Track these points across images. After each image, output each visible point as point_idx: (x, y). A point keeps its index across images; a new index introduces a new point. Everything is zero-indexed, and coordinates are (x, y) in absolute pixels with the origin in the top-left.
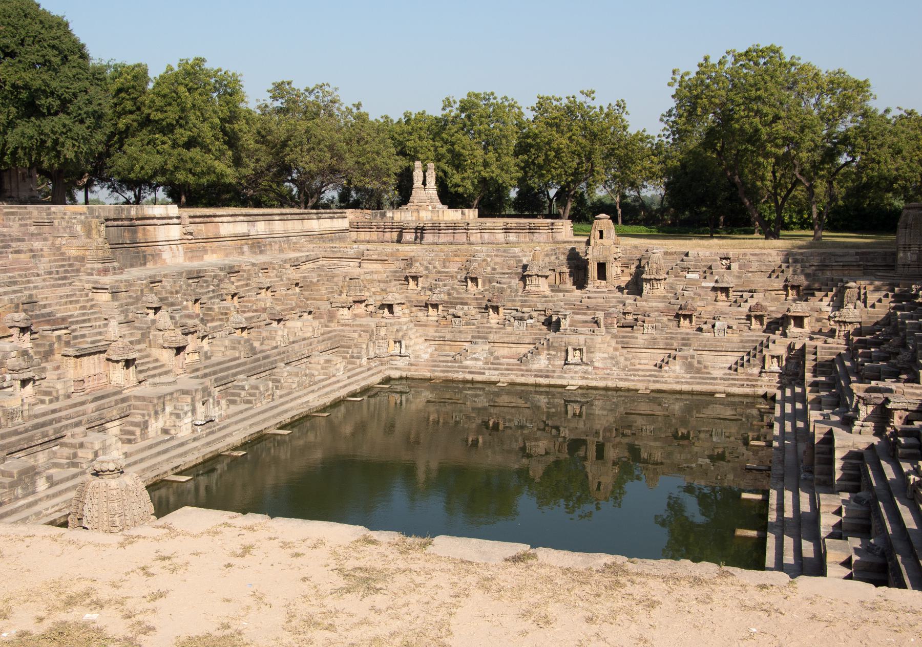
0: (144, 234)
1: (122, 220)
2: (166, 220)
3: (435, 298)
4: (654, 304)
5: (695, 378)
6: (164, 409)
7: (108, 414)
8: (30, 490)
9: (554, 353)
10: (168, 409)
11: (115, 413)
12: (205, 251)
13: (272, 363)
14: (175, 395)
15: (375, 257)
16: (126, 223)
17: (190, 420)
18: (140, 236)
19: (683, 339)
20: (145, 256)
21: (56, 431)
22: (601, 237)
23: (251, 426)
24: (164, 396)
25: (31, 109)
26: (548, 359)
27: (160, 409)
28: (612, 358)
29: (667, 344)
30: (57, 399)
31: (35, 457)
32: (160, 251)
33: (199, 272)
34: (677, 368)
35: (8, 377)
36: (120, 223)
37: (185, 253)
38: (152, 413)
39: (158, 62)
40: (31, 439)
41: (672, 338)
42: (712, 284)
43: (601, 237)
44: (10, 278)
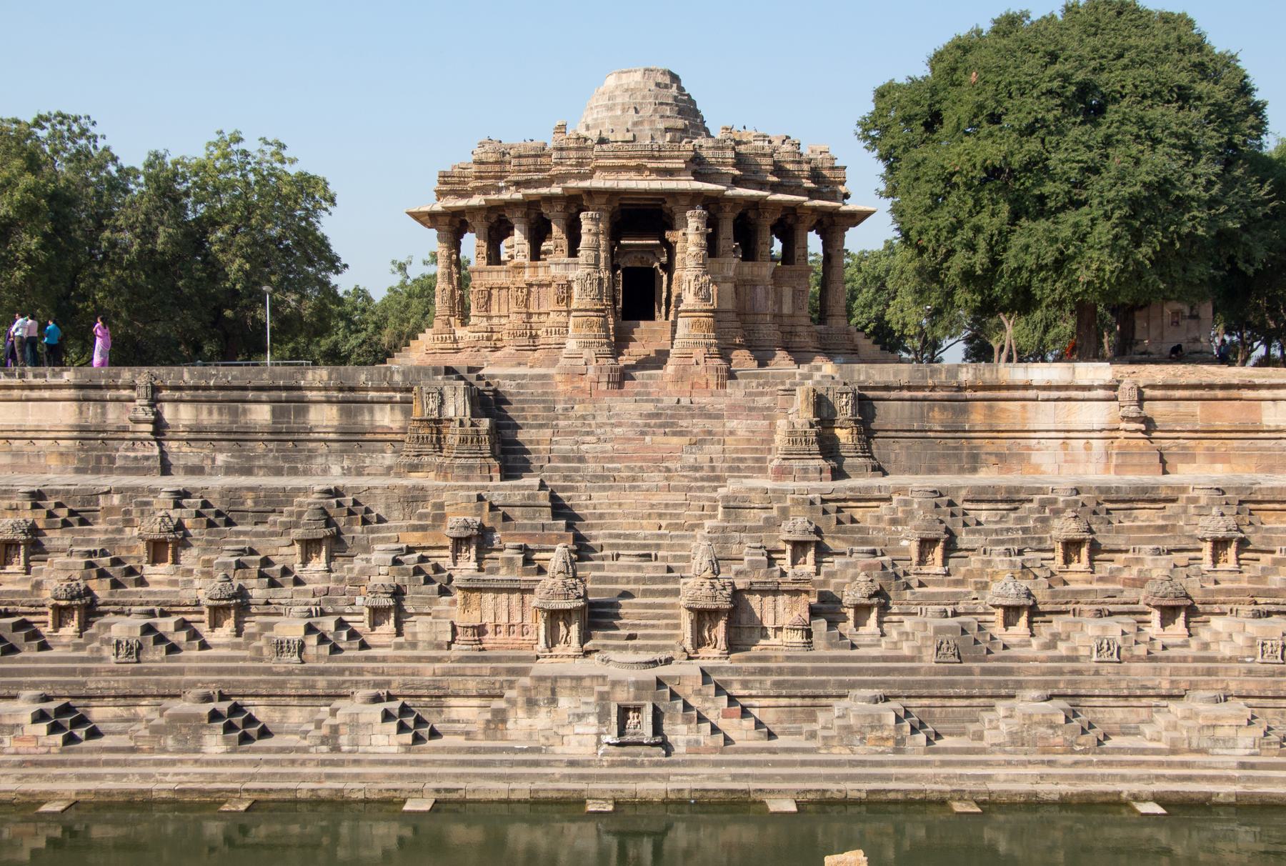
0: (991, 413)
1: (933, 388)
2: (1065, 392)
6: (553, 701)
7: (454, 684)
8: (191, 744)
10: (565, 703)
11: (472, 685)
12: (1188, 457)
13: (1005, 684)
14: (587, 683)
16: (939, 394)
17: (594, 730)
18: (977, 416)
21: (330, 684)
23: (735, 777)
24: (555, 679)
25: (1027, 207)
27: (542, 698)
30: (414, 645)
31: (285, 712)
32: (1029, 448)
33: (1018, 490)
35: (359, 600)
36: (920, 394)
37: (1108, 455)
38: (521, 700)
39: (187, 145)
40: (282, 684)
44: (609, 470)
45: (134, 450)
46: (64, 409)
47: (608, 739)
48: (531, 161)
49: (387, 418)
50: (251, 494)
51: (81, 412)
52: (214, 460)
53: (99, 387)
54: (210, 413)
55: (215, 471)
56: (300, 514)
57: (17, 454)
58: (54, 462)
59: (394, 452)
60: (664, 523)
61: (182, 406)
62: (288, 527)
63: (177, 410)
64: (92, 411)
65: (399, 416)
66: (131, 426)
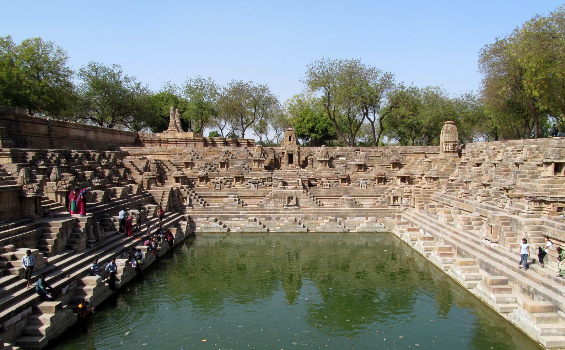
3: (201, 173)
4: (325, 174)
5: (356, 210)
6: (67, 232)
9: (277, 200)
15: (162, 153)
19: (345, 191)
20: (26, 142)
22: (290, 140)
26: (274, 204)
28: (310, 201)
29: (337, 193)
34: (346, 205)
41: (339, 190)
42: (353, 163)
43: (290, 140)
47: (92, 241)
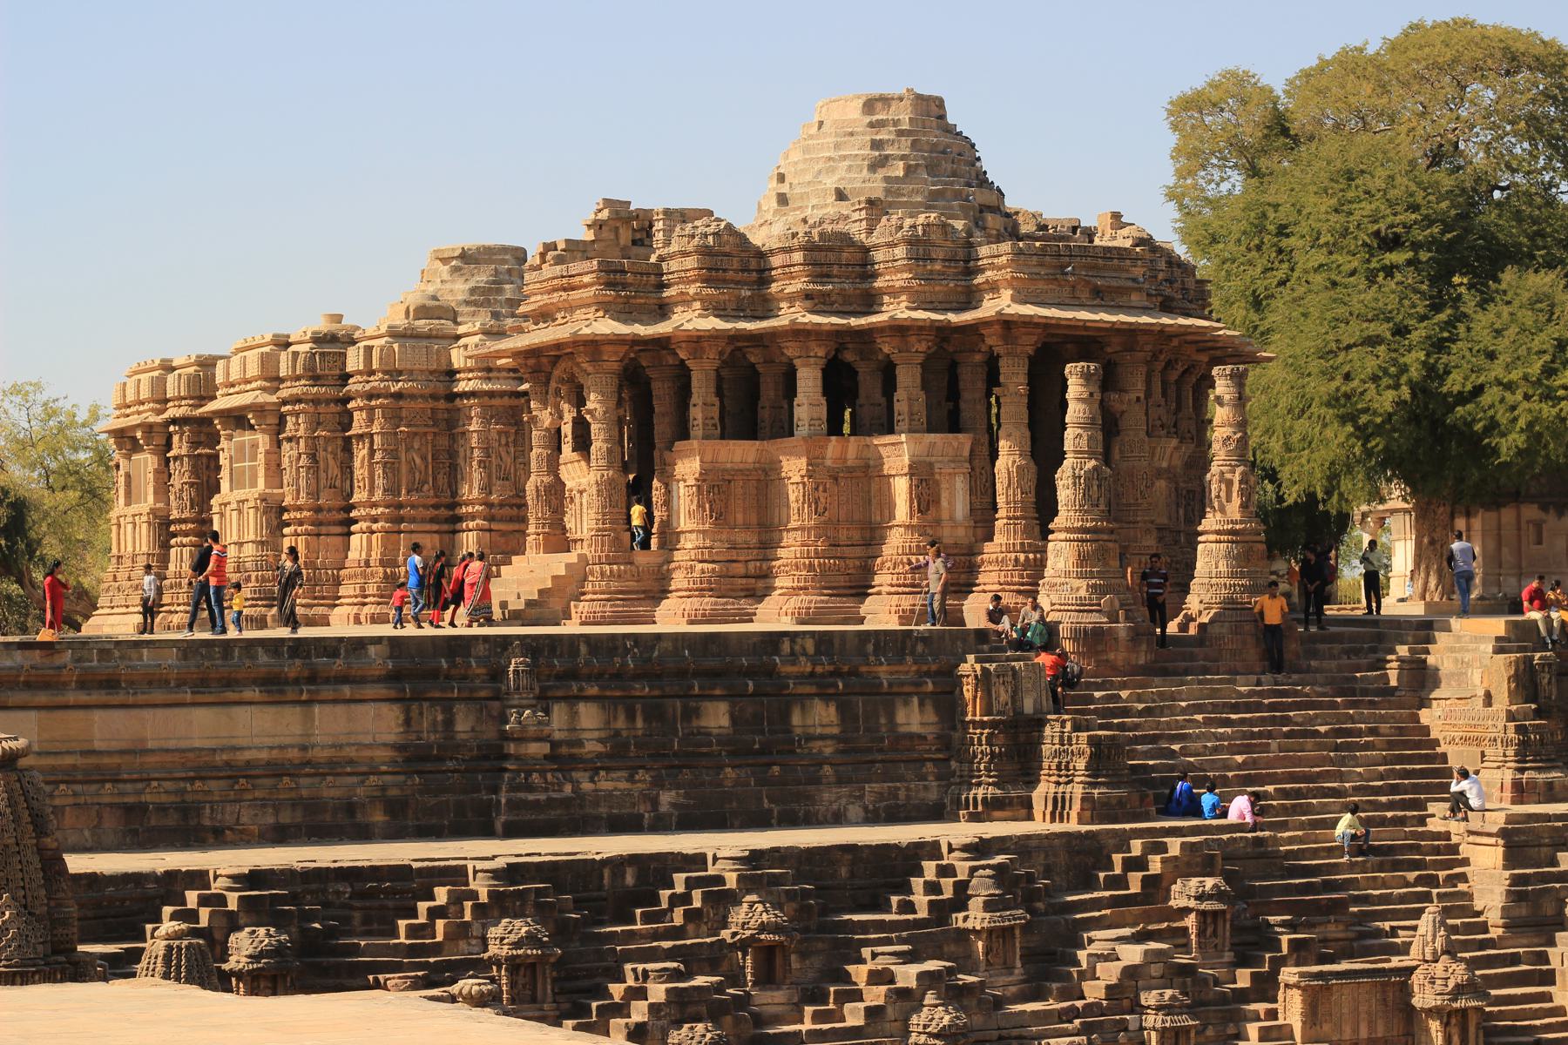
45: (530, 788)
46: (378, 716)
48: (832, 257)
49: (913, 719)
50: (848, 857)
51: (407, 722)
52: (655, 803)
53: (434, 674)
54: (631, 717)
55: (660, 826)
56: (962, 887)
57: (312, 806)
58: (379, 817)
59: (938, 778)
60: (1412, 876)
61: (582, 707)
62: (941, 911)
63: (574, 715)
64: (429, 718)
65: (931, 717)
66: (511, 748)
